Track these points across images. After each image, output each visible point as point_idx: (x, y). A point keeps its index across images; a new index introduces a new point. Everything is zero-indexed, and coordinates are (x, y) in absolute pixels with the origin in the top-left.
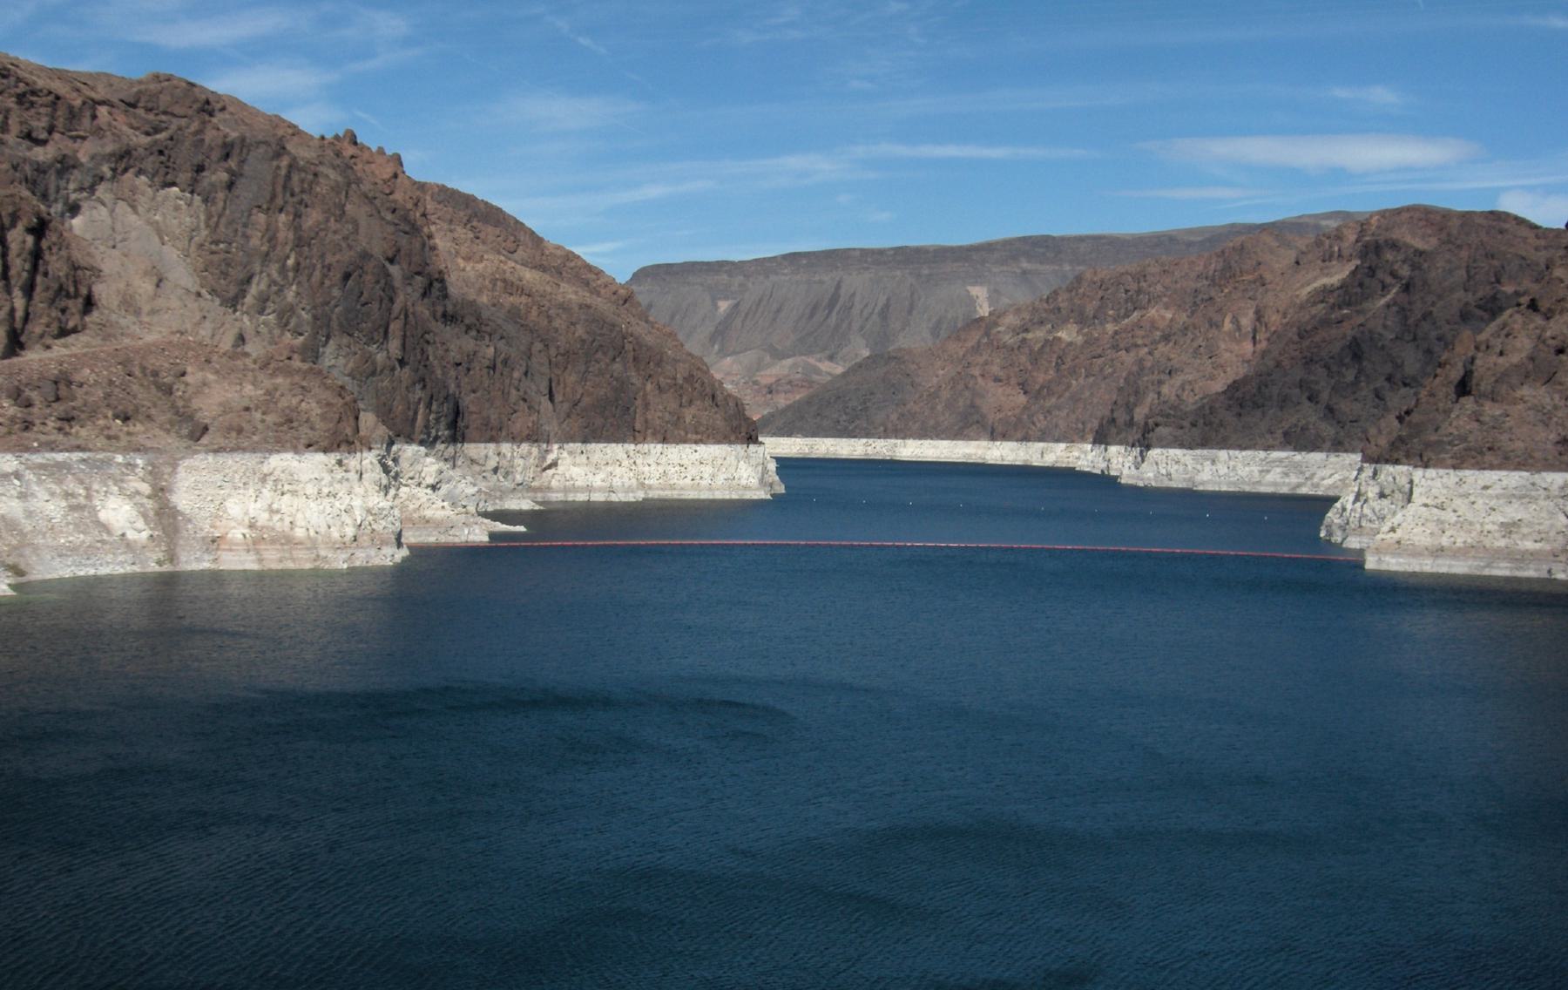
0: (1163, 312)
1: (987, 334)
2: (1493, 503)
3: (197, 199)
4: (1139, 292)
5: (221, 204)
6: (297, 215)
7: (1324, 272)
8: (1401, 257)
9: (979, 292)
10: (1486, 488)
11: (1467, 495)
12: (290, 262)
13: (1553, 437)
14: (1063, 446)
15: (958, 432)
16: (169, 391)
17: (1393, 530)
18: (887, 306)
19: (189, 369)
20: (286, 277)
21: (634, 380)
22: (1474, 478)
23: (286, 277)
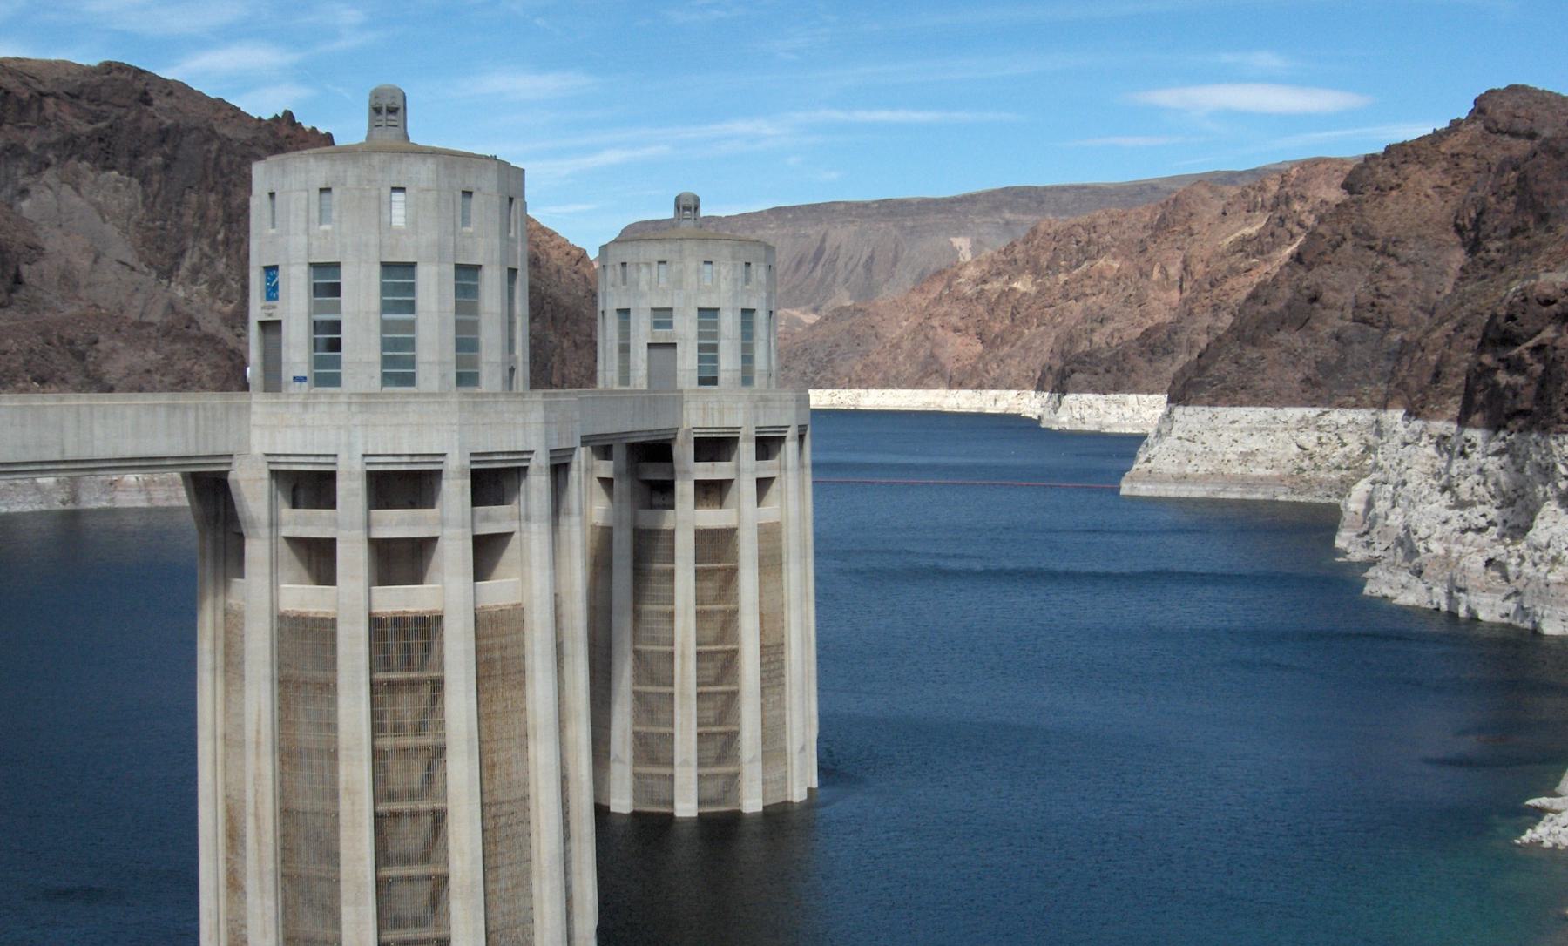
0: (1111, 262)
1: (949, 286)
2: (1236, 436)
3: (135, 181)
4: (1089, 242)
5: (156, 186)
6: (227, 194)
7: (1247, 222)
8: (1307, 208)
9: (962, 243)
10: (1233, 422)
11: (1215, 430)
12: (220, 237)
13: (1299, 376)
14: (1014, 393)
15: (917, 384)
16: (82, 356)
17: (1148, 460)
18: (871, 258)
19: (102, 338)
20: (216, 250)
21: (552, 338)
22: (1225, 413)
23: (216, 250)
